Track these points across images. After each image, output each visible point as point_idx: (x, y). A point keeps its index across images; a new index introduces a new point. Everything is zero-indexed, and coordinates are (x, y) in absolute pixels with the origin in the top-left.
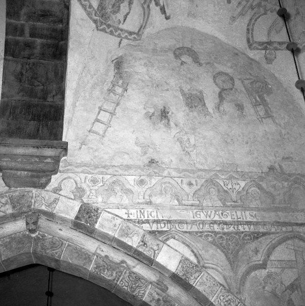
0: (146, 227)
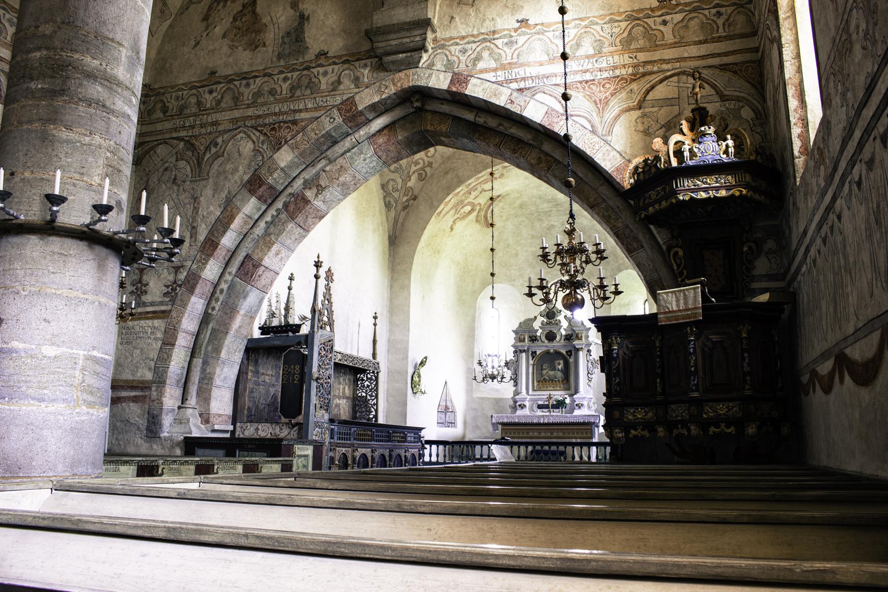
0: (514, 86)
